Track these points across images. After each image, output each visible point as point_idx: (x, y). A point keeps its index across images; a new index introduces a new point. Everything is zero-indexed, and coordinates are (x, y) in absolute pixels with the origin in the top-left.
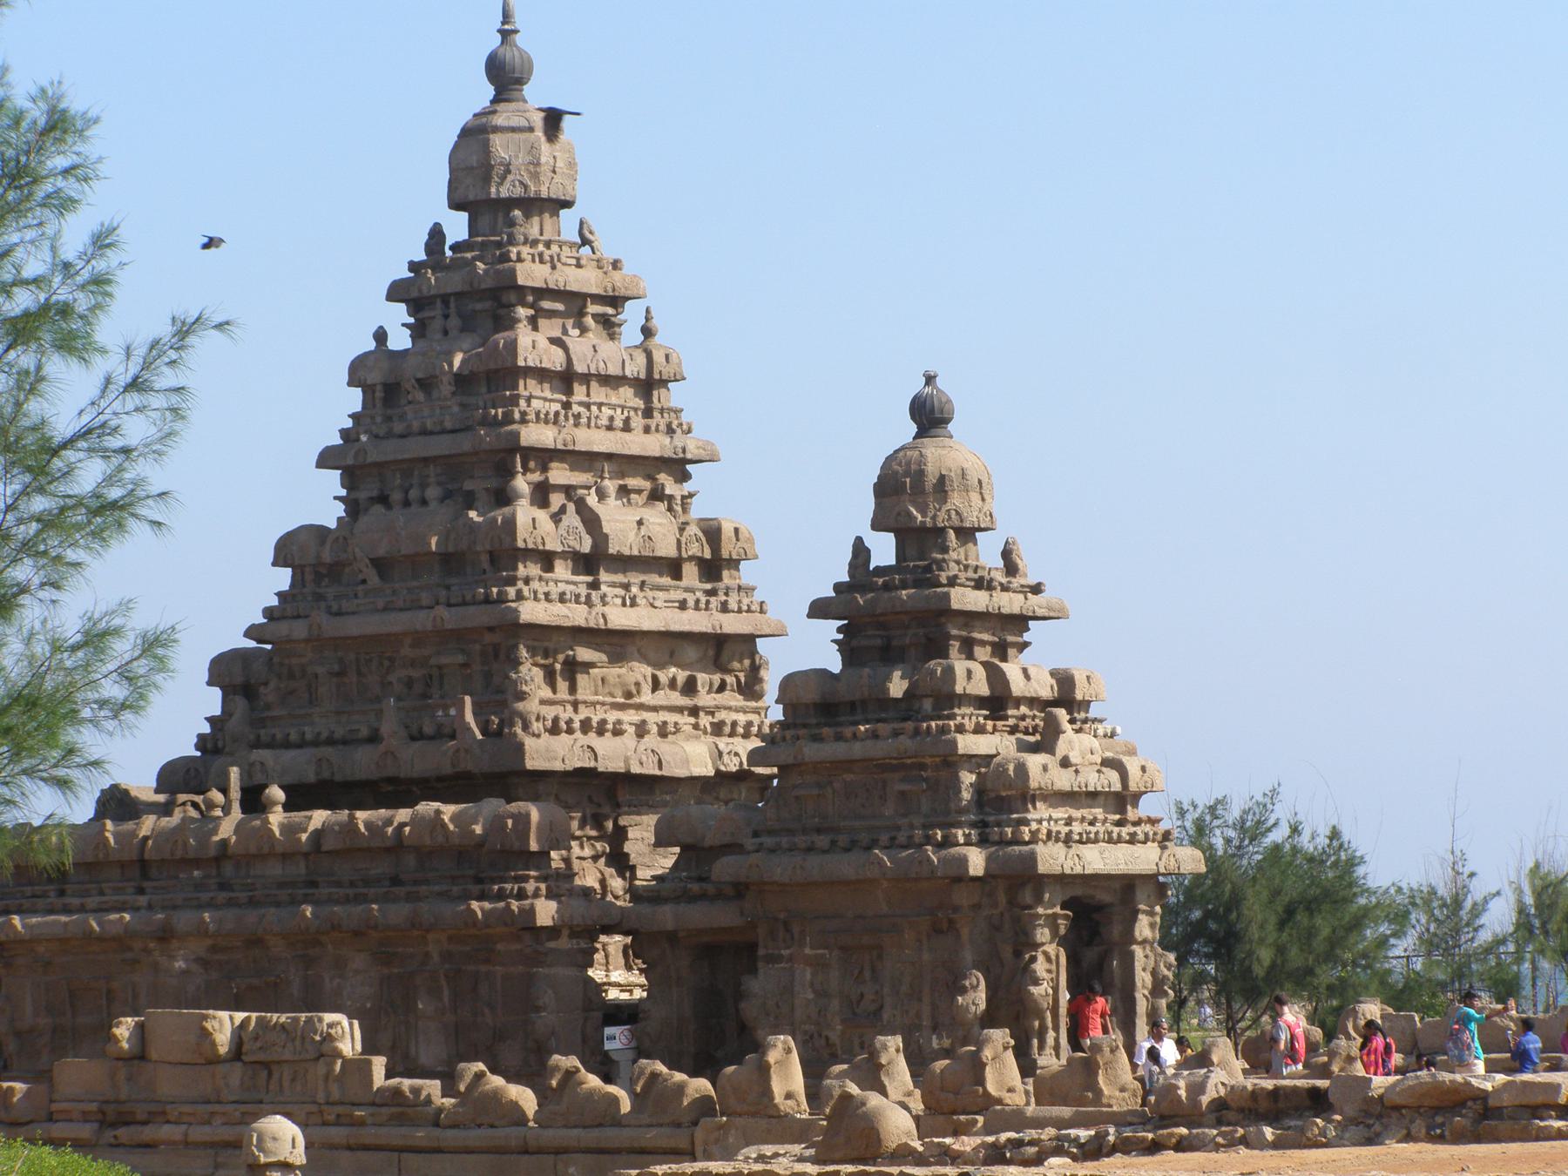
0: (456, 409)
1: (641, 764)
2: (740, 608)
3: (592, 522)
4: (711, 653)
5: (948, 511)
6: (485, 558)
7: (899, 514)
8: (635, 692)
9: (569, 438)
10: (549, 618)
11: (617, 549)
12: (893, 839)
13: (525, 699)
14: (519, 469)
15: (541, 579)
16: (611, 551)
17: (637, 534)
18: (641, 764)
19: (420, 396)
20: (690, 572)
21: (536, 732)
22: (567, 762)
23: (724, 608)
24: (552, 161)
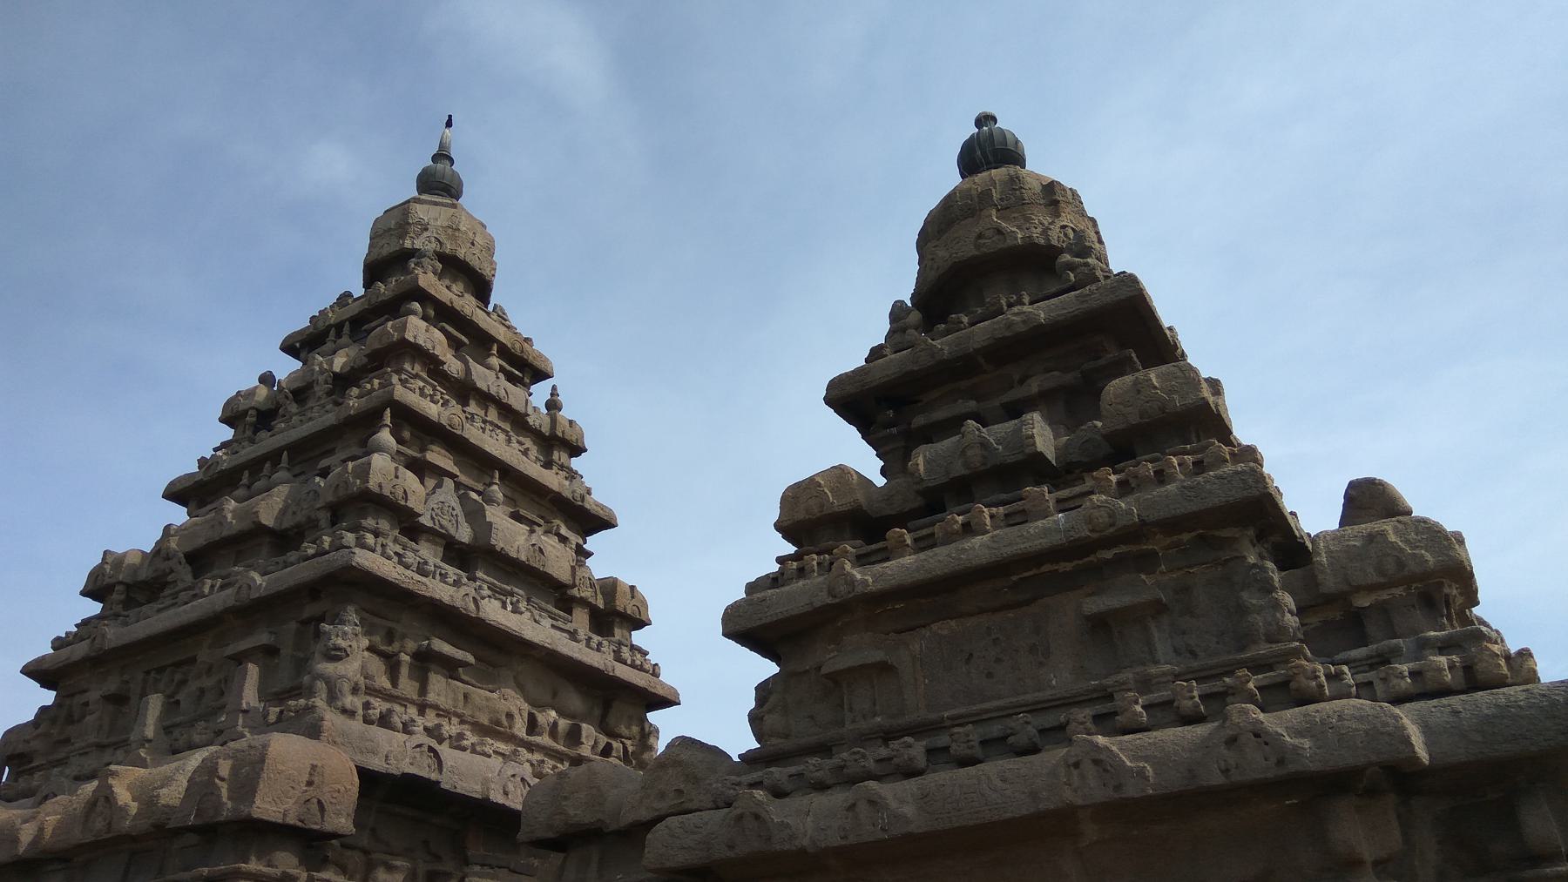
0: (329, 407)
1: (506, 793)
2: (633, 661)
3: (475, 515)
4: (597, 712)
5: (1064, 227)
6: (324, 517)
7: (980, 236)
8: (506, 723)
9: (456, 420)
10: (398, 577)
11: (502, 546)
12: (1097, 718)
13: (337, 659)
14: (388, 421)
15: (396, 541)
16: (493, 542)
17: (527, 540)
18: (506, 793)
19: (294, 408)
20: (580, 620)
21: (348, 706)
22: (392, 761)
23: (619, 658)
24: (471, 235)
